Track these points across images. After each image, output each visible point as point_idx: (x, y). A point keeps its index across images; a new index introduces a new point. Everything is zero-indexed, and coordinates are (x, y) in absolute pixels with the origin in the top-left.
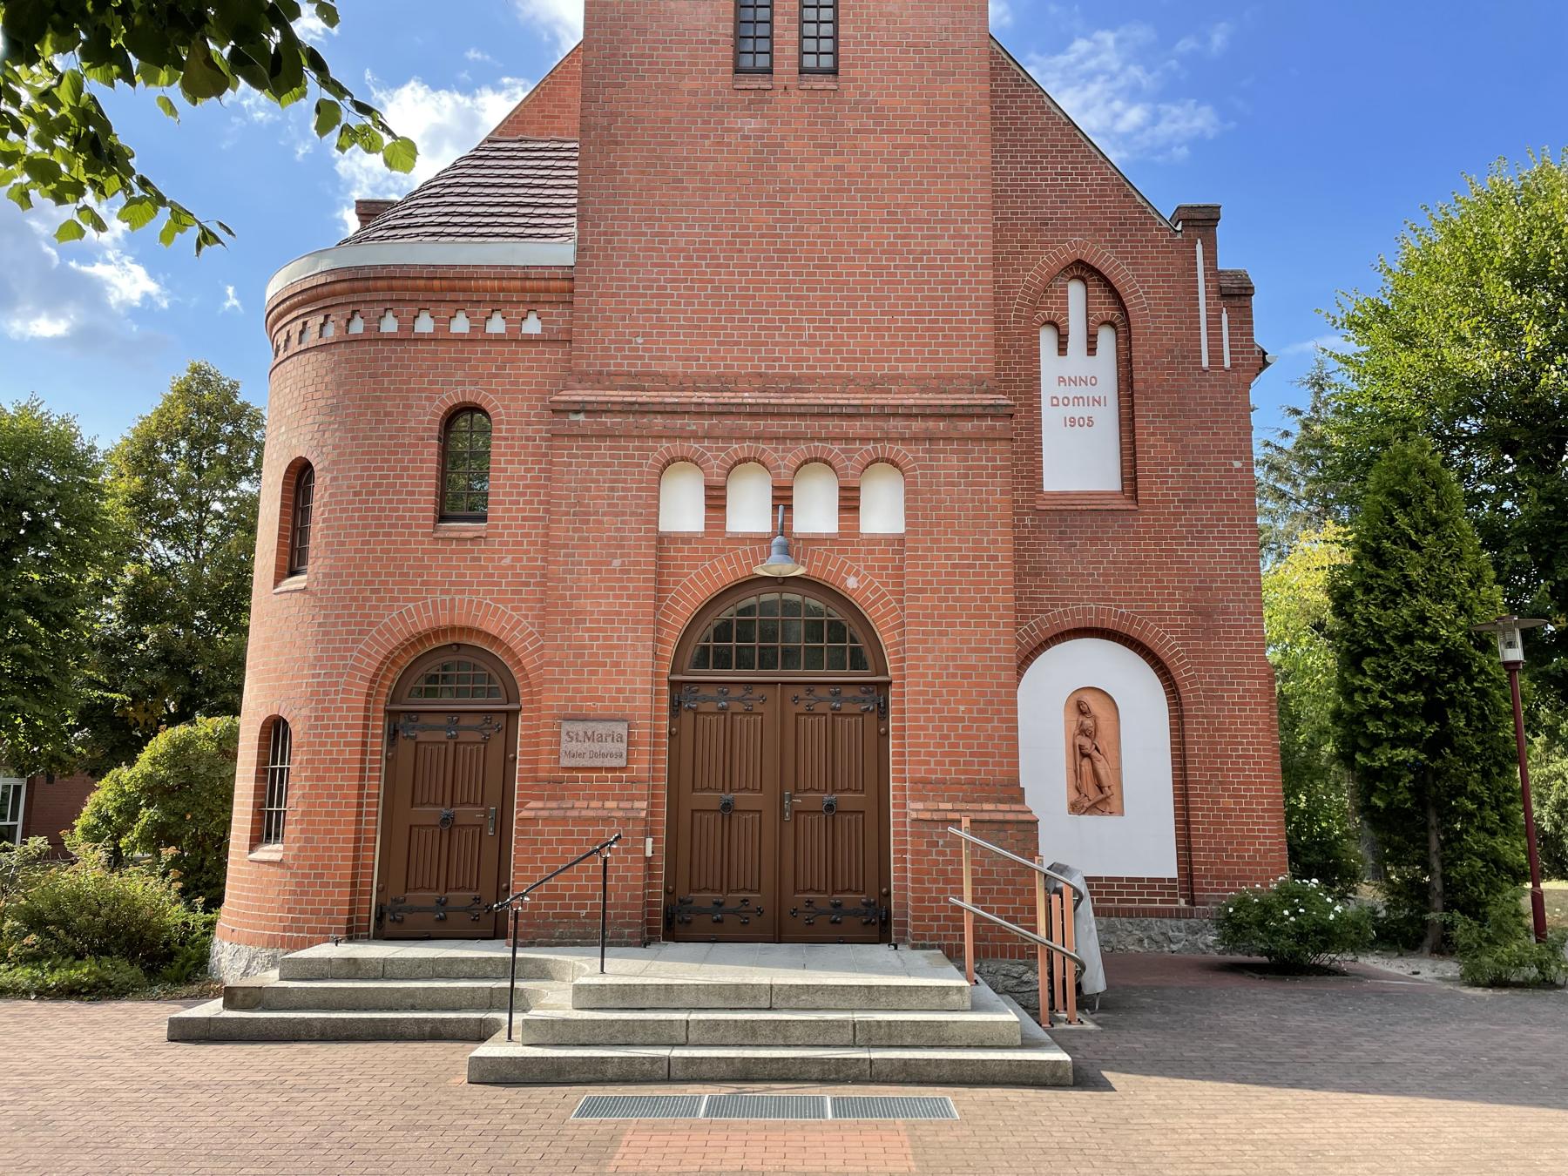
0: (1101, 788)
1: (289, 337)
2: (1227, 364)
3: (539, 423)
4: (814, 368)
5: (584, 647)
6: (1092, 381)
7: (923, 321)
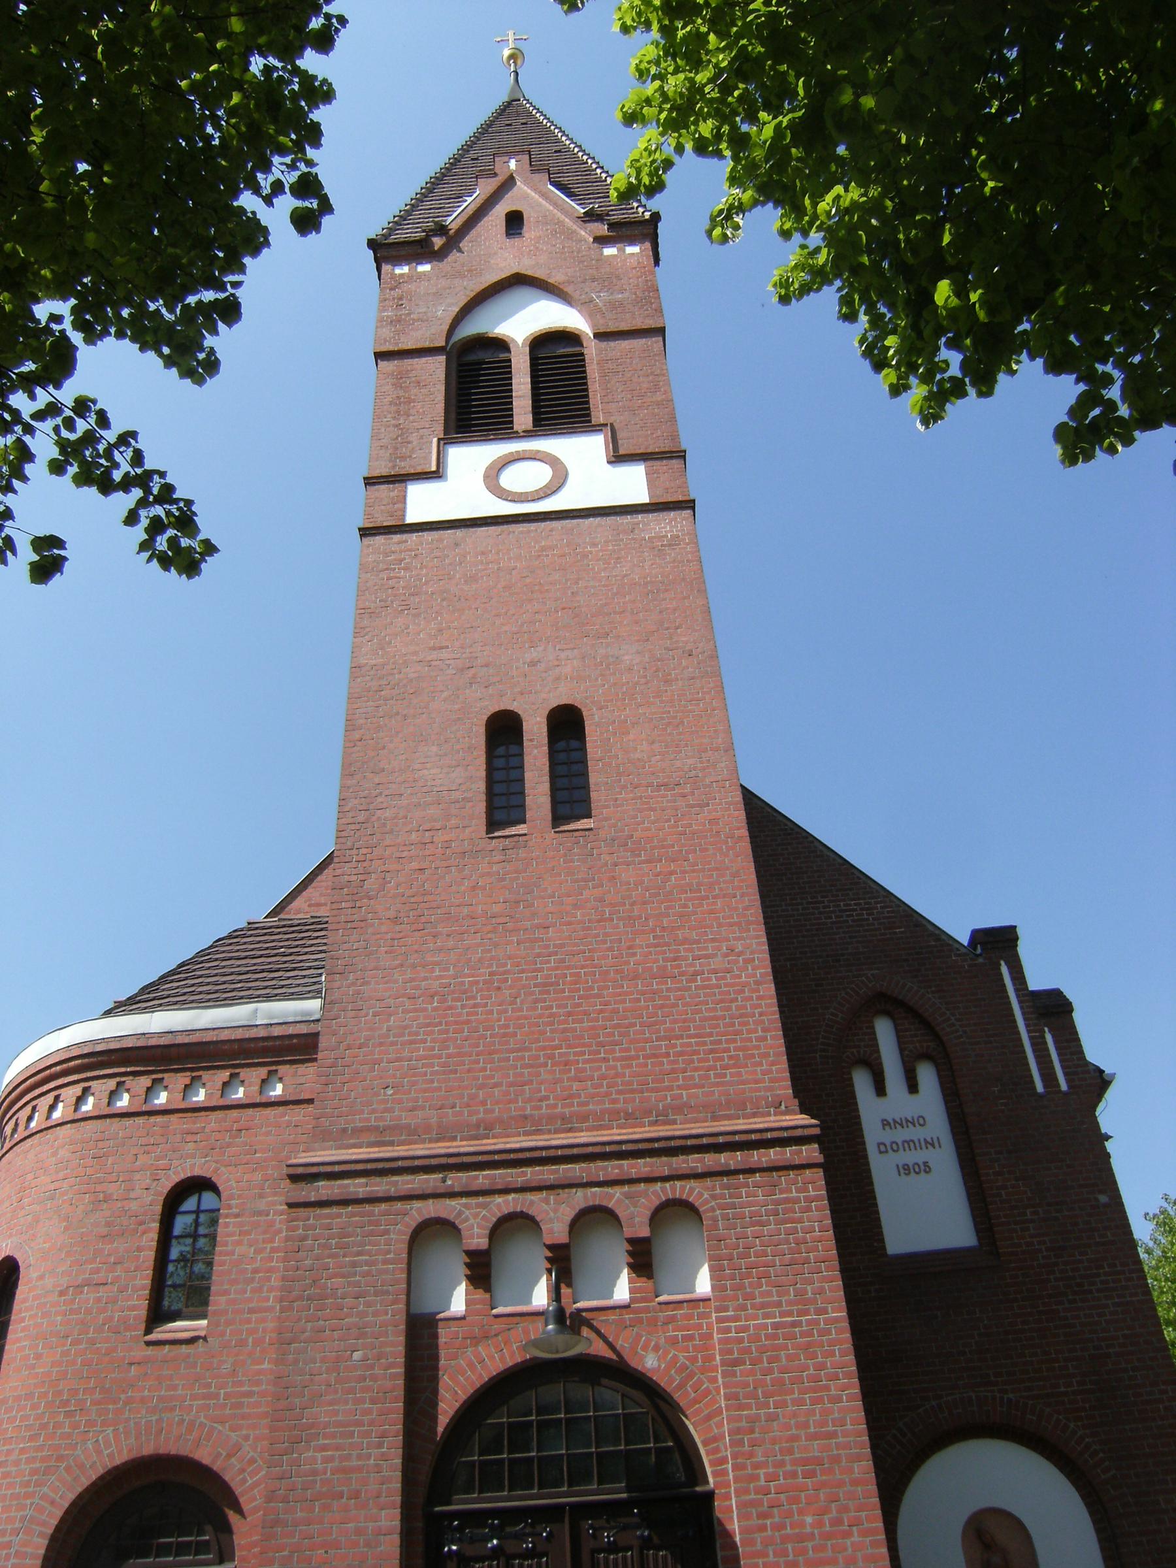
1: (17, 1124)
2: (1064, 1086)
3: (275, 1194)
4: (586, 1104)
5: (315, 1473)
6: (920, 1121)
7: (704, 1043)
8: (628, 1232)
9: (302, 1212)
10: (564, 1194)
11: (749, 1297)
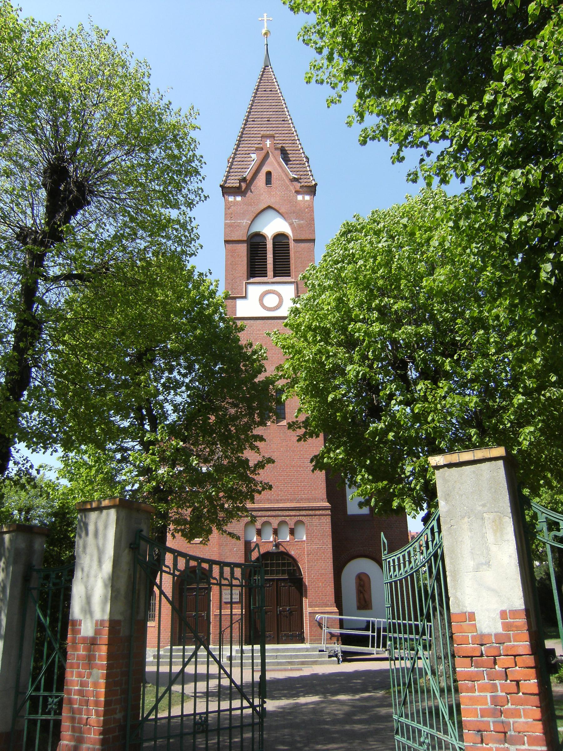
0: (365, 602)
8: (289, 527)
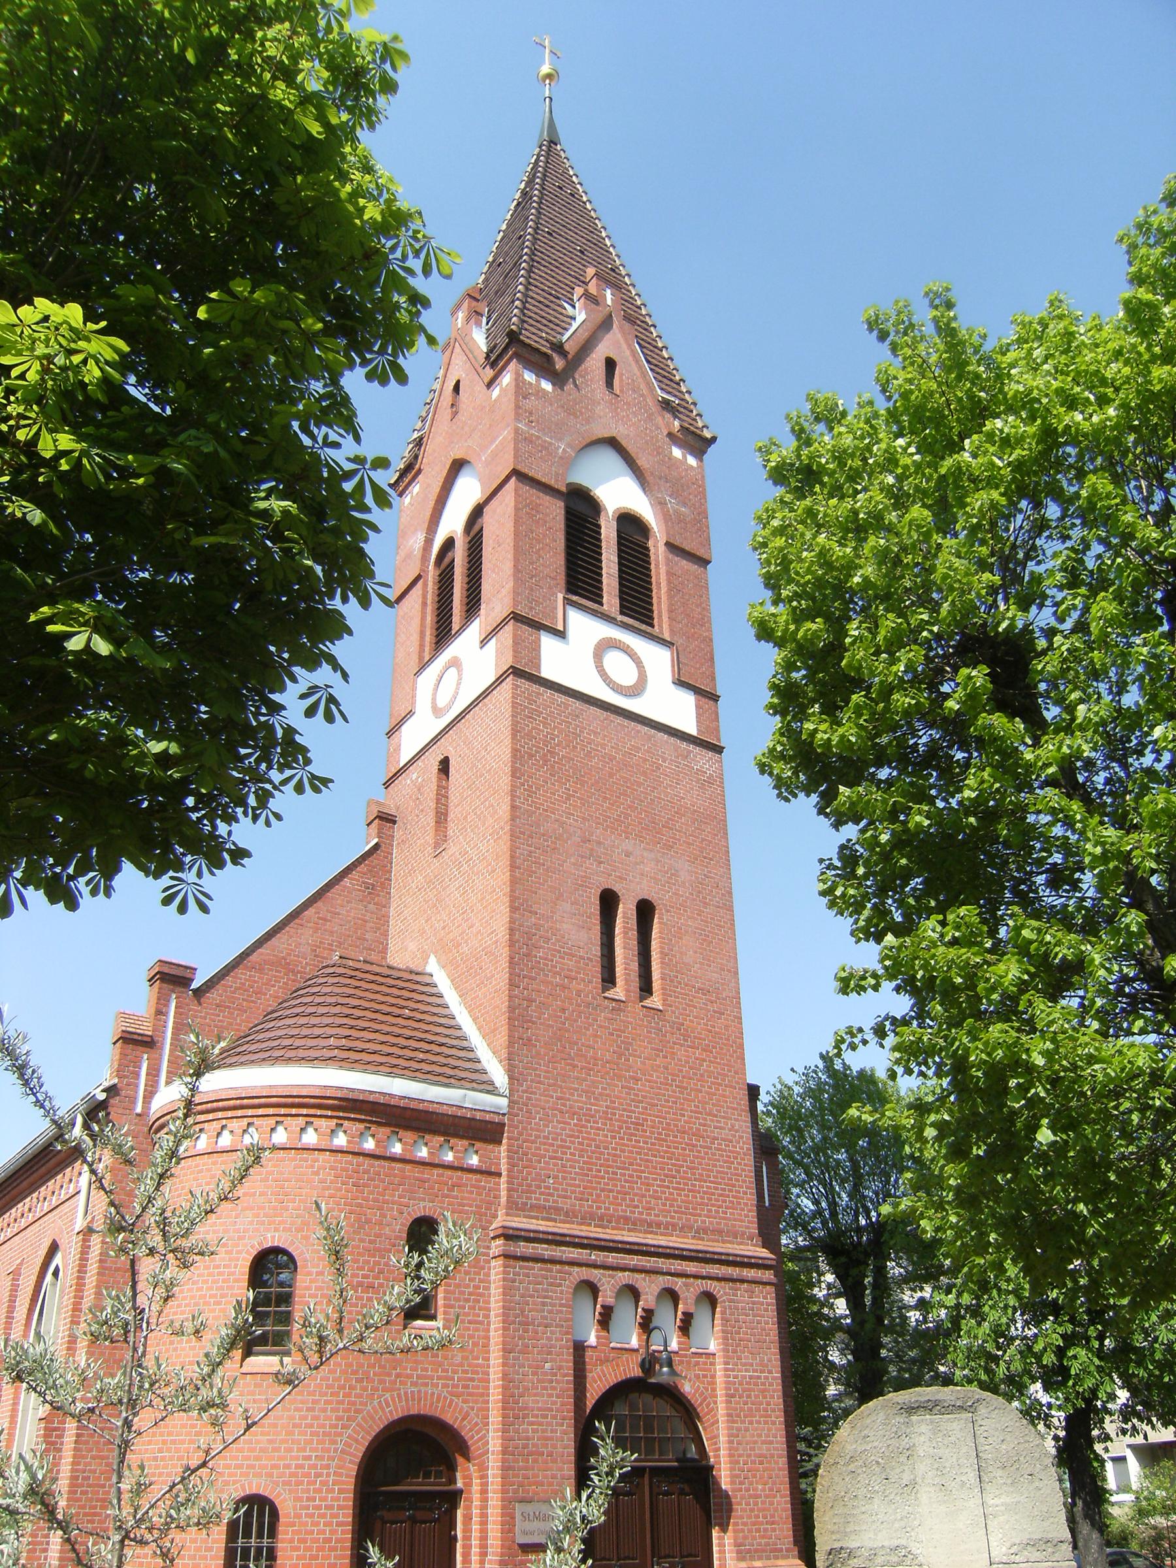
5: (528, 1439)
9: (512, 1262)
10: (653, 1277)
11: (739, 1358)
